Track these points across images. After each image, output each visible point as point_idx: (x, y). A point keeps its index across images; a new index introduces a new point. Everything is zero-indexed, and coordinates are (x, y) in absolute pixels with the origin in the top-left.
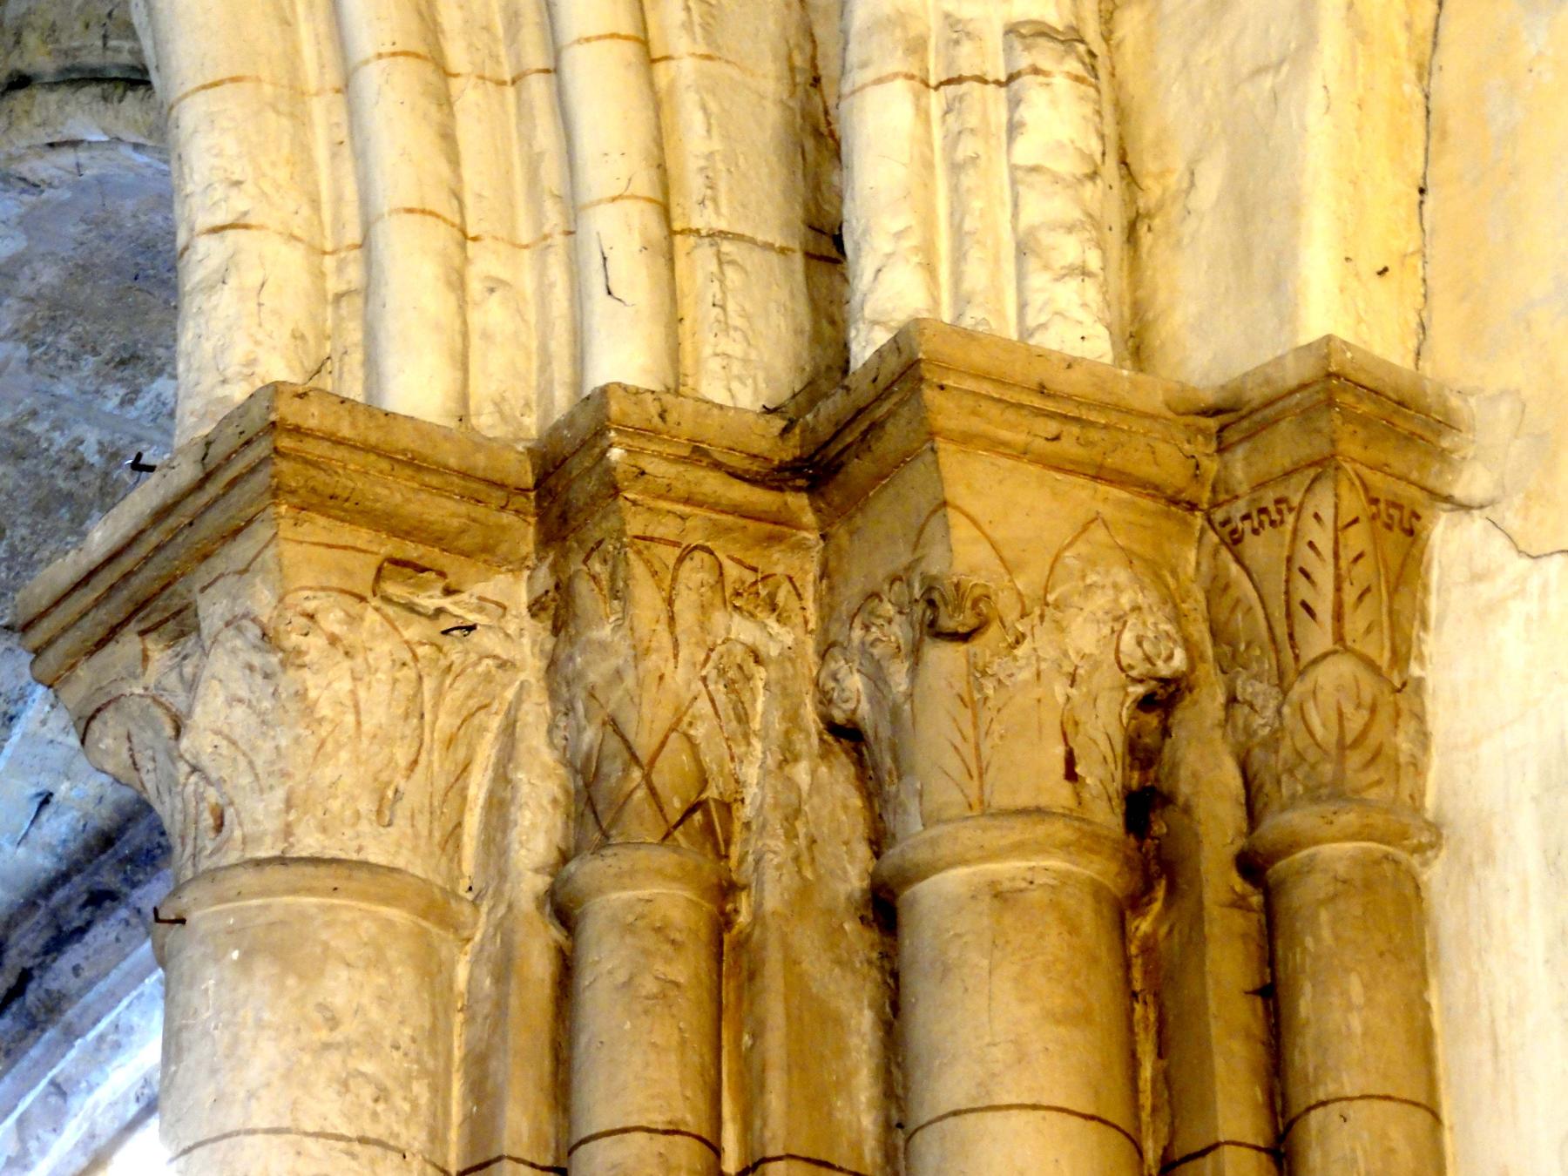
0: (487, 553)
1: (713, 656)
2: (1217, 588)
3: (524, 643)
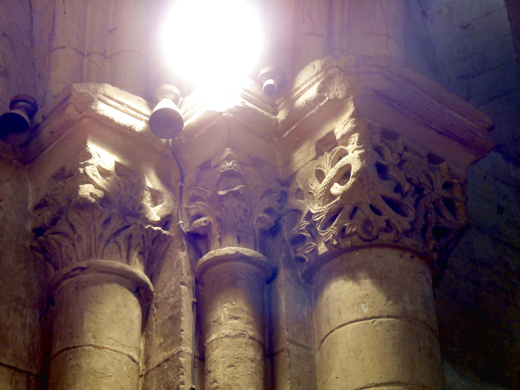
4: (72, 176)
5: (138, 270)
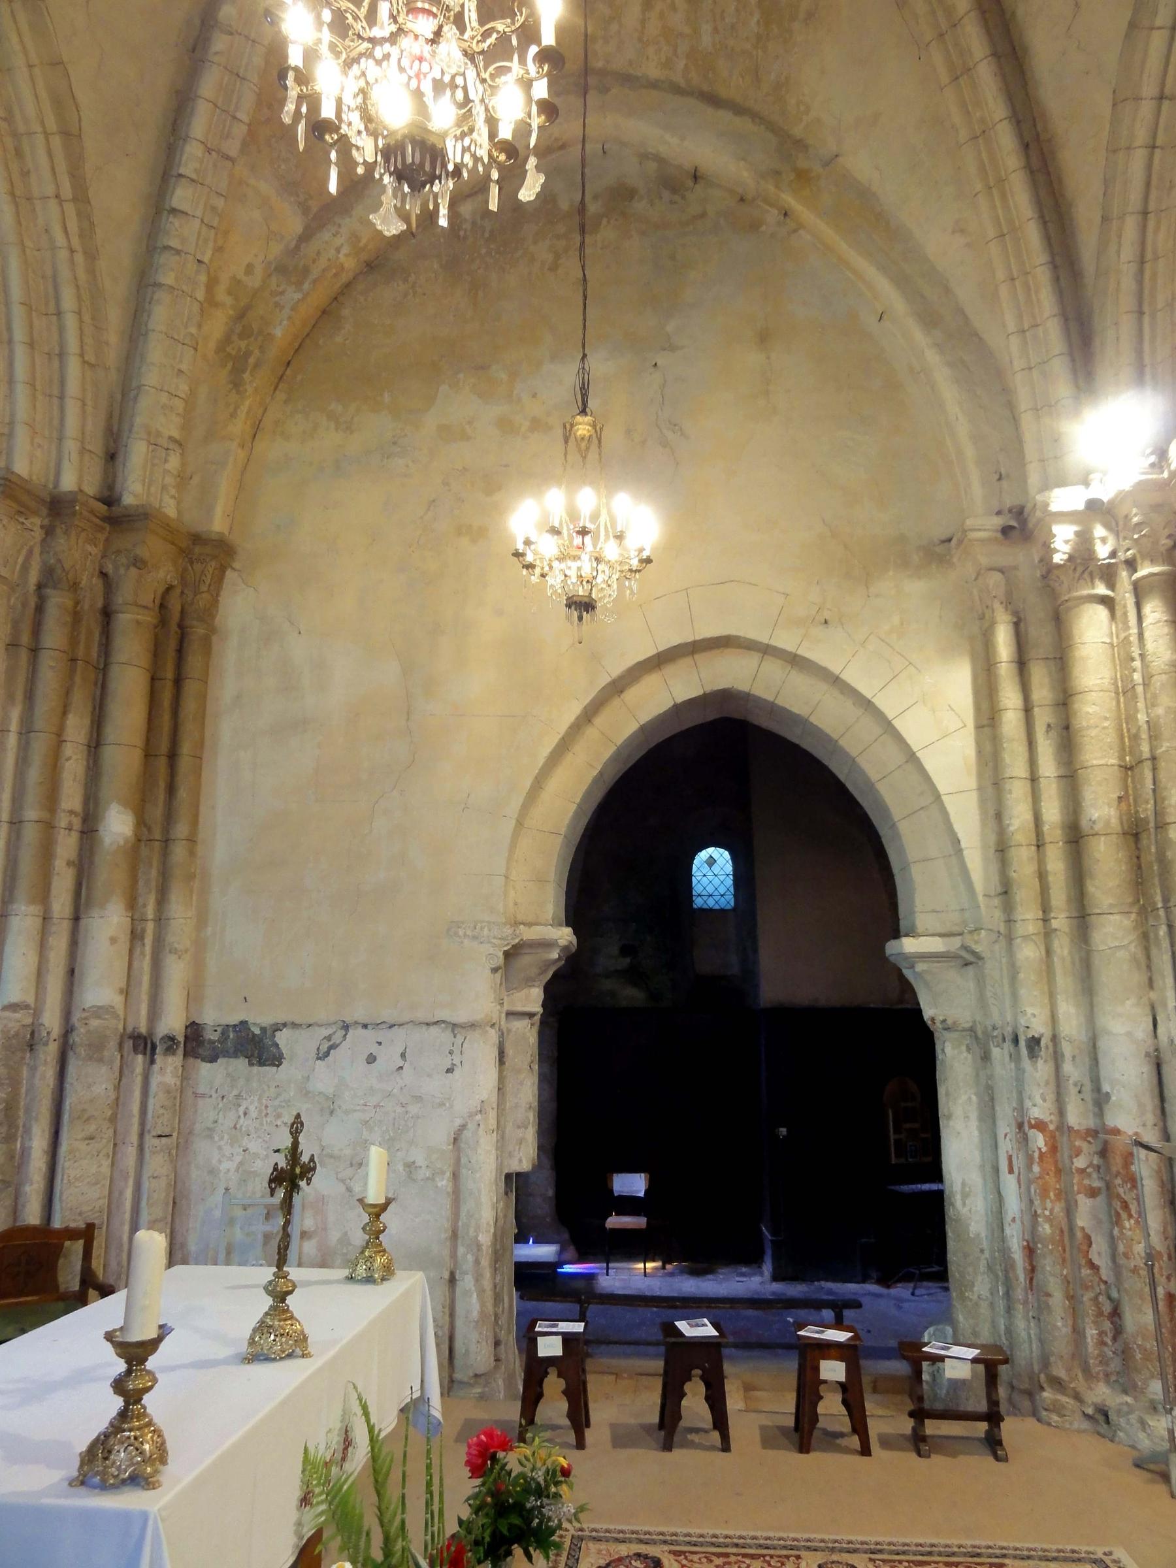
0: (35, 513)
1: (78, 551)
2: (185, 570)
3: (38, 534)
4: (1048, 550)
5: (1101, 589)
